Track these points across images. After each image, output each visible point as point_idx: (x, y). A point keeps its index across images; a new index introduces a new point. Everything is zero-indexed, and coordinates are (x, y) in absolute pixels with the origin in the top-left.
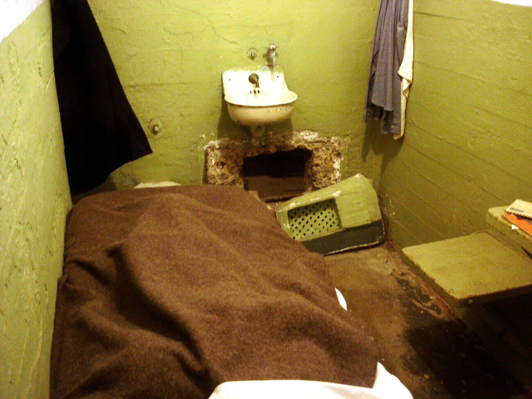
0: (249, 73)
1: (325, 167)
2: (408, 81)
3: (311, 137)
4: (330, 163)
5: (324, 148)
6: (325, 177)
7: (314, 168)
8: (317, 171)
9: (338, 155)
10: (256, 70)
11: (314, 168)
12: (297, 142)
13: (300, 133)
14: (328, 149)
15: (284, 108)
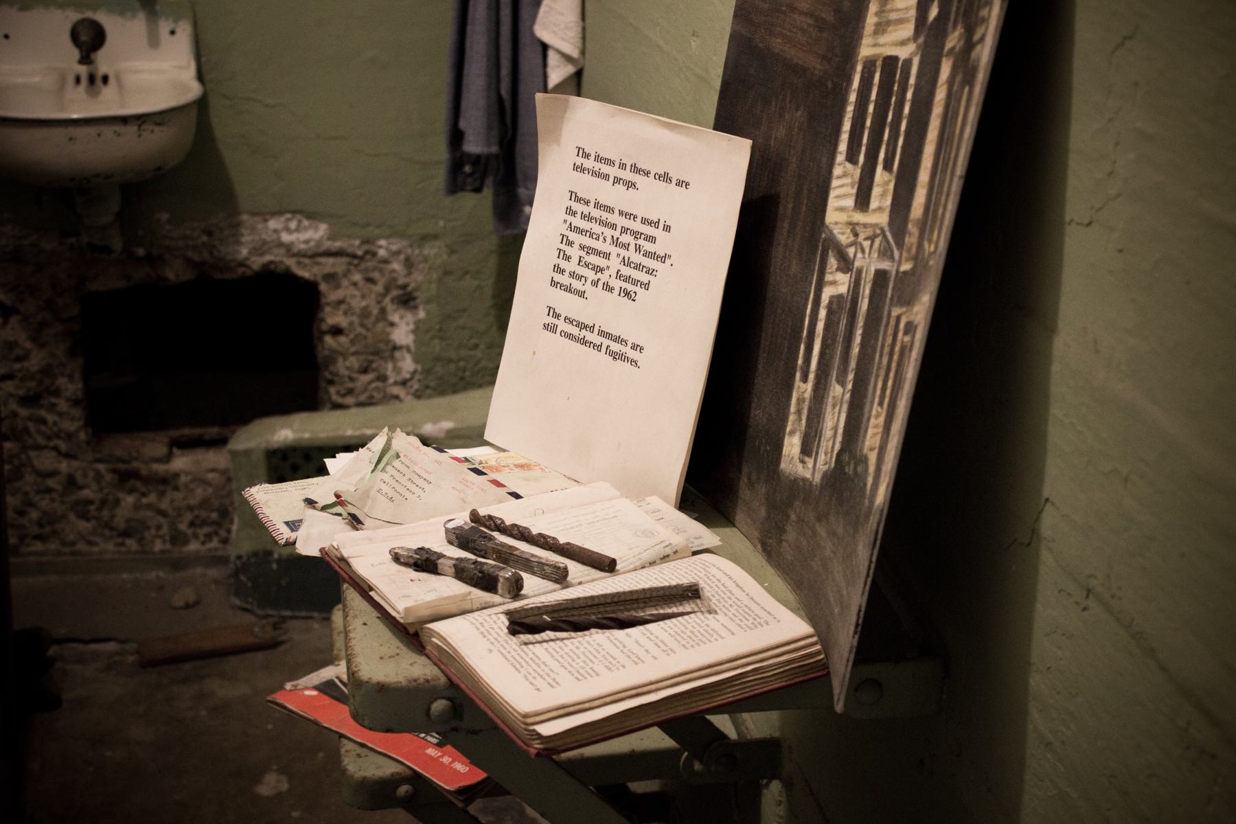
0: (74, 16)
1: (365, 338)
2: (568, 58)
3: (309, 234)
4: (380, 326)
5: (357, 277)
6: (365, 371)
7: (328, 339)
8: (336, 352)
9: (407, 300)
10: (95, 8)
11: (328, 339)
12: (259, 250)
13: (266, 221)
14: (370, 280)
15: (132, 129)
